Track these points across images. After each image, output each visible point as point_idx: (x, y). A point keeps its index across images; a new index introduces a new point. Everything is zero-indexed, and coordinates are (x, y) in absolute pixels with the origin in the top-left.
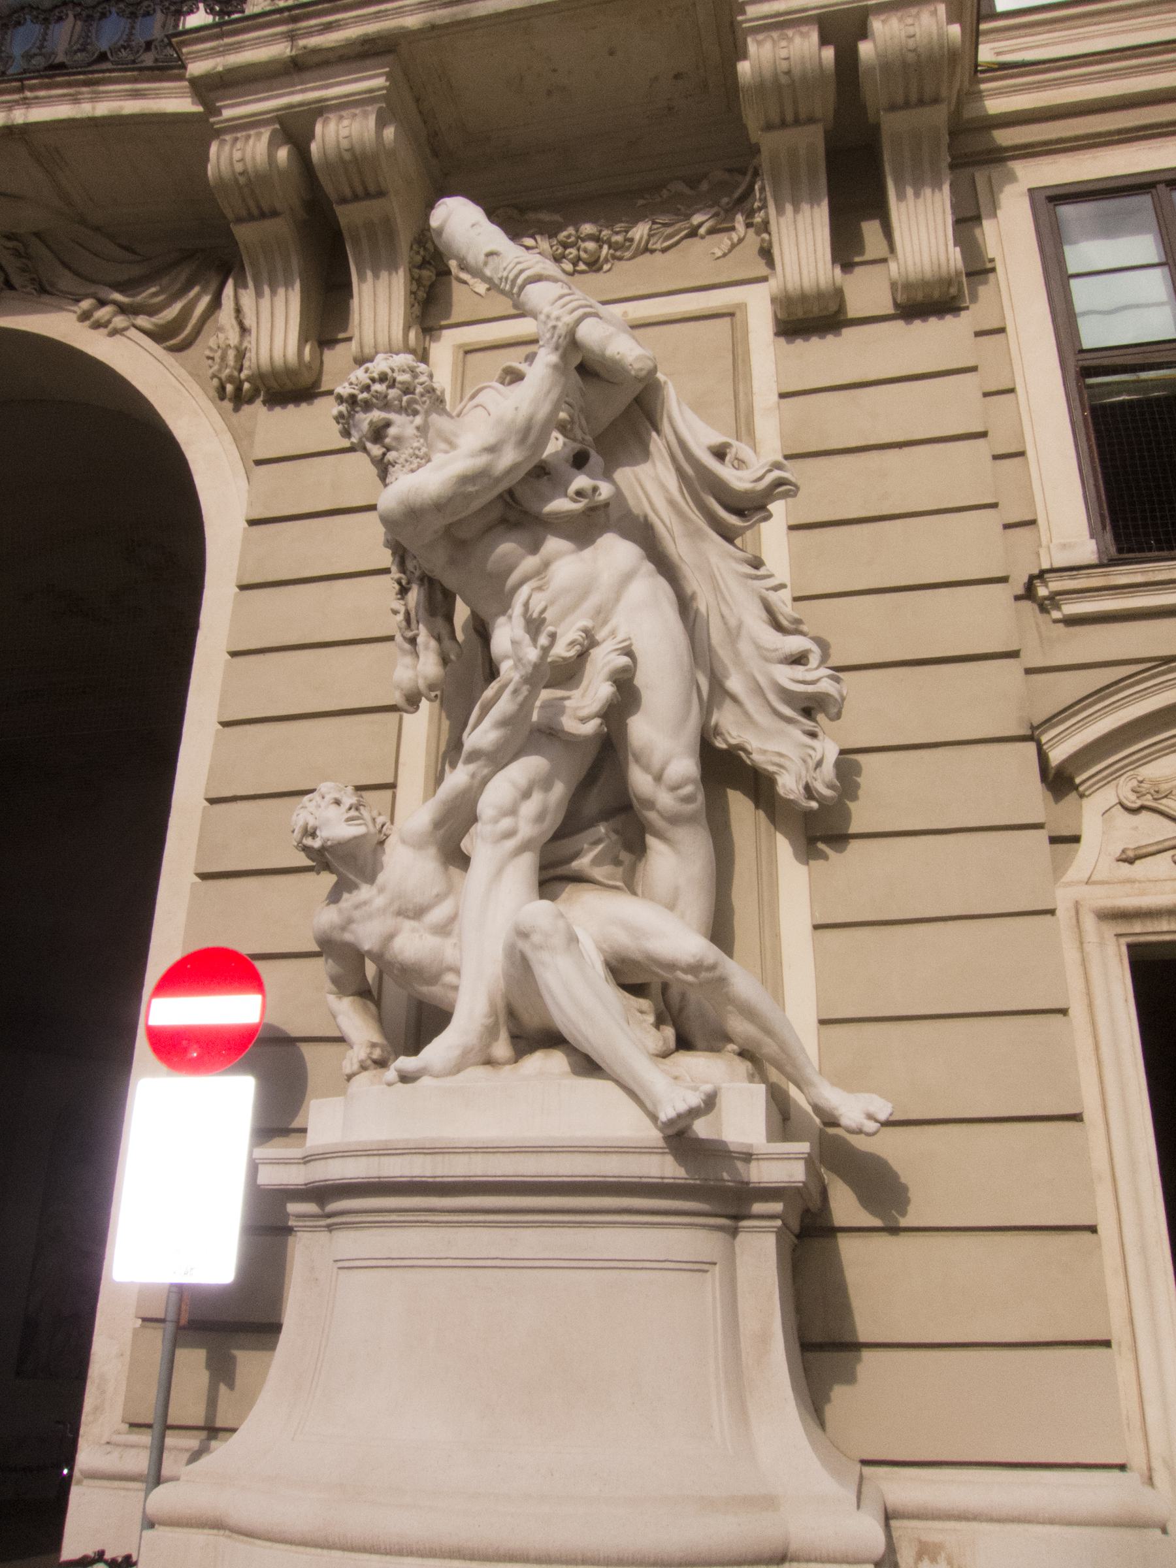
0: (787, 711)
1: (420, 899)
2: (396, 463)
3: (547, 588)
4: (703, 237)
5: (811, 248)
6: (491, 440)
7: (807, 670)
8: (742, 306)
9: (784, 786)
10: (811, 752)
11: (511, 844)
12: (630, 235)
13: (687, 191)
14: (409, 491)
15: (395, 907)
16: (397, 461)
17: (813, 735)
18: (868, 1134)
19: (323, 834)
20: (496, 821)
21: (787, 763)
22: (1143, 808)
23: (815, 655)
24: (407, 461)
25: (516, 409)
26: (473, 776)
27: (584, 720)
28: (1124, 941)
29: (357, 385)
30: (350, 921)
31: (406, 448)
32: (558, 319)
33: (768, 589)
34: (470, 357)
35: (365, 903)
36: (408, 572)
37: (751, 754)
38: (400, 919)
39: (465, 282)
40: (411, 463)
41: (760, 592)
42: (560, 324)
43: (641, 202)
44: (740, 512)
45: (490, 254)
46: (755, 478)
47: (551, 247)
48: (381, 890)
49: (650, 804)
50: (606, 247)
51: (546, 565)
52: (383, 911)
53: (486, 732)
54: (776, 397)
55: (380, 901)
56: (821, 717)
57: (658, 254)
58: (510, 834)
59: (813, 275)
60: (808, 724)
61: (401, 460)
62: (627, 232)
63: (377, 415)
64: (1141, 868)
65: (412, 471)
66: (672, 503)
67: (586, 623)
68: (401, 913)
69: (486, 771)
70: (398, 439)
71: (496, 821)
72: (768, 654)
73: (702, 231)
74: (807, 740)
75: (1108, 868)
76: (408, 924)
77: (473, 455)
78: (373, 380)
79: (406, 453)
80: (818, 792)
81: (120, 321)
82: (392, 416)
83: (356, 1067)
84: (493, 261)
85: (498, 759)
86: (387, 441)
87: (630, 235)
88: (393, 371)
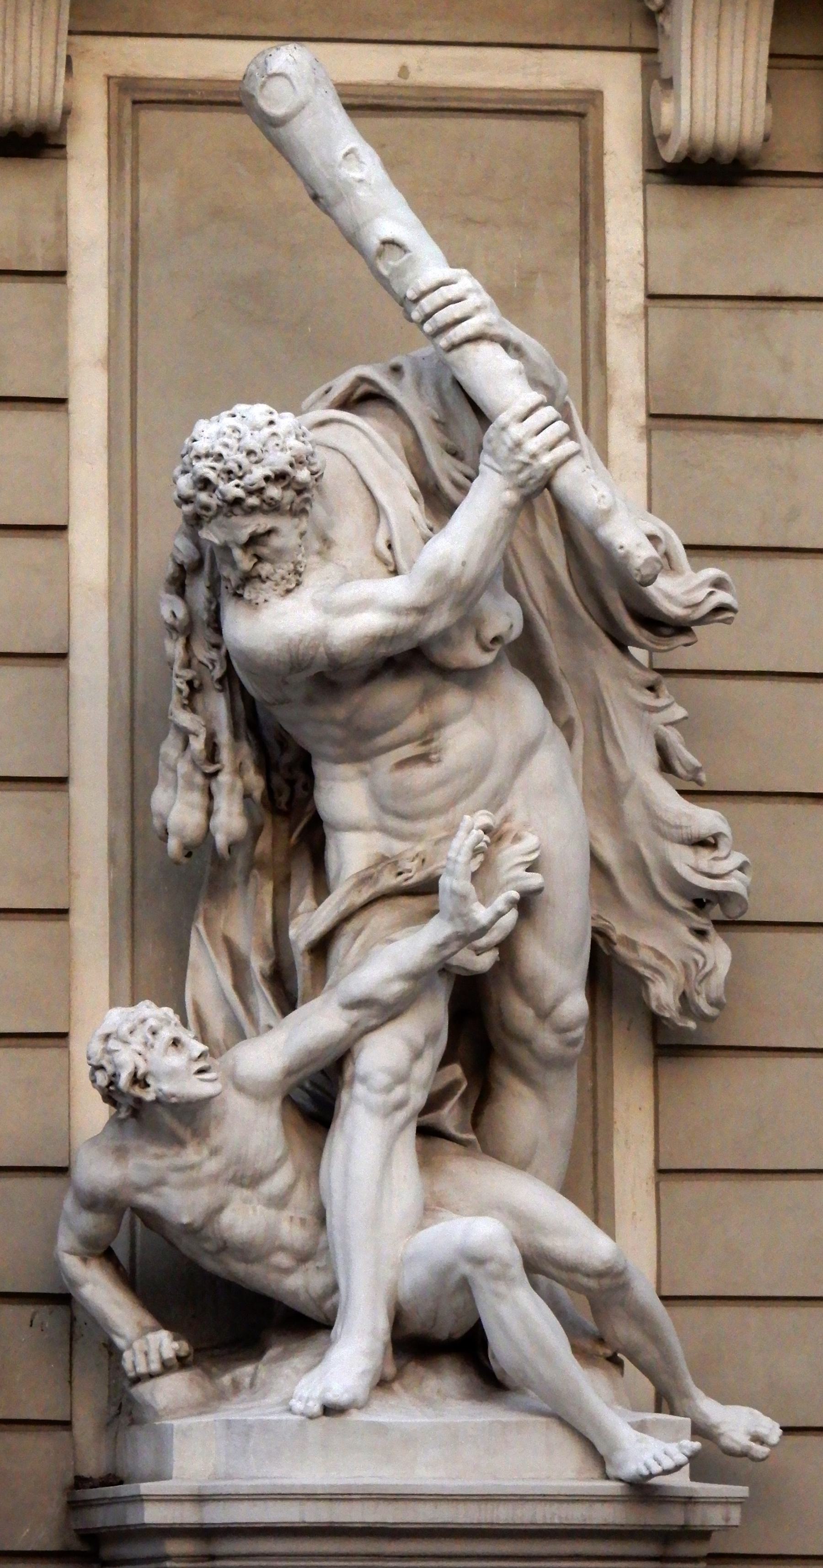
1: (262, 1164)
2: (267, 578)
3: (439, 761)
5: (737, 78)
6: (426, 599)
7: (715, 859)
8: (594, 97)
9: (658, 999)
10: (698, 957)
11: (401, 1116)
14: (301, 641)
15: (231, 1173)
16: (272, 578)
17: (701, 934)
18: (754, 1459)
20: (388, 1089)
21: (666, 968)
23: (726, 839)
24: (283, 578)
25: (464, 564)
26: (355, 1025)
27: (479, 951)
29: (241, 478)
30: (160, 1182)
31: (287, 562)
32: (534, 456)
33: (665, 725)
35: (192, 1167)
36: (195, 662)
37: (615, 944)
38: (231, 1187)
40: (288, 581)
41: (658, 729)
42: (536, 464)
45: (390, 243)
46: (687, 603)
49: (525, 1041)
51: (437, 726)
52: (215, 1178)
53: (389, 981)
54: (639, 298)
55: (212, 1166)
58: (400, 1105)
59: (735, 124)
61: (277, 577)
63: (260, 523)
65: (288, 591)
66: (552, 583)
67: (484, 818)
69: (373, 1022)
70: (280, 552)
71: (388, 1089)
72: (665, 828)
74: (693, 940)
76: (246, 1193)
78: (267, 479)
79: (284, 568)
80: (698, 1008)
82: (284, 524)
83: (155, 1367)
86: (264, 551)
88: (291, 465)
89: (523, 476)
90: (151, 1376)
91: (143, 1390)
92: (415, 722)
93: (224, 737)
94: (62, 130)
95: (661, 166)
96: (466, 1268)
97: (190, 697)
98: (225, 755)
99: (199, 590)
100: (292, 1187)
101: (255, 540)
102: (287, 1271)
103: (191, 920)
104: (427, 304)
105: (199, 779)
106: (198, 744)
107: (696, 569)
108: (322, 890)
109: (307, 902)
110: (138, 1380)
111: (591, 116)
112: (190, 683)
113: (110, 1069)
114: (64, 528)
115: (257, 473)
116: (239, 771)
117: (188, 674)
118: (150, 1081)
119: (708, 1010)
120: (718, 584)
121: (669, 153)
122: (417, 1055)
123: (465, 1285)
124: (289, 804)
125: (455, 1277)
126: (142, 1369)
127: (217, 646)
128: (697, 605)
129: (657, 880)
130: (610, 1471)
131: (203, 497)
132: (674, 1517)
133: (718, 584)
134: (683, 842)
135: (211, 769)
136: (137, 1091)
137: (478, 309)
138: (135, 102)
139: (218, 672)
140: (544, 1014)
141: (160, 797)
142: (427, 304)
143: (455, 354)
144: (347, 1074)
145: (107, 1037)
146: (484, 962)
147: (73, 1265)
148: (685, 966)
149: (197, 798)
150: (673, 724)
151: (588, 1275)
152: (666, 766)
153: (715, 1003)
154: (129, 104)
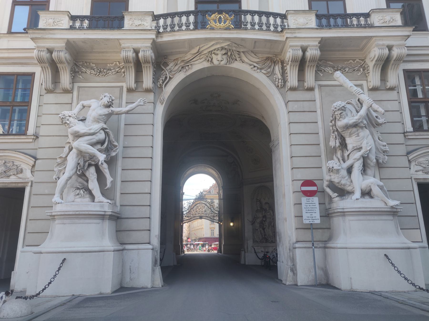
0: (381, 152)
4: (356, 71)
6: (359, 118)
8: (362, 84)
12: (345, 69)
13: (353, 62)
17: (384, 155)
19: (335, 168)
21: (381, 159)
22: (419, 165)
27: (365, 154)
28: (416, 182)
30: (335, 178)
34: (322, 87)
39: (318, 73)
43: (346, 63)
44: (377, 125)
47: (333, 70)
48: (340, 175)
49: (369, 164)
50: (342, 71)
55: (340, 176)
56: (385, 153)
57: (349, 73)
58: (359, 169)
60: (384, 154)
62: (345, 69)
64: (418, 173)
65: (344, 119)
68: (342, 178)
73: (356, 70)
75: (414, 173)
76: (344, 179)
77: (356, 119)
80: (384, 162)
81: (258, 70)
82: (343, 112)
83: (335, 197)
84: (351, 88)
85: (358, 160)
87: (345, 69)
89: (369, 105)
90: (335, 198)
91: (334, 199)
92: (357, 133)
93: (337, 136)
94: (314, 88)
95: (369, 89)
96: (370, 184)
97: (333, 132)
98: (337, 138)
99: (333, 122)
100: (348, 179)
101: (340, 114)
102: (348, 187)
103: (333, 155)
104: (356, 91)
105: (335, 140)
106: (334, 137)
107: (382, 119)
108: (348, 151)
109: (346, 151)
110: (333, 198)
111: (362, 86)
112: (333, 131)
113: (329, 167)
114: (317, 122)
115: (341, 106)
116: (338, 139)
117: (333, 130)
118: (334, 167)
119: (385, 162)
120: (385, 120)
121: (370, 88)
122: (361, 164)
123: (370, 186)
124: (342, 144)
125: (369, 185)
126: (334, 197)
127: (335, 127)
128: (383, 122)
129: (380, 150)
130: (388, 205)
131: (335, 109)
132: (395, 210)
133: (385, 120)
134: (382, 146)
135: (336, 139)
136: (332, 169)
137: (361, 91)
138: (320, 86)
139: (336, 130)
140: (372, 161)
141: (330, 143)
142: (356, 91)
143: (359, 95)
144: (353, 167)
145: (329, 164)
146: (366, 155)
147: (325, 188)
148: (383, 158)
149: (334, 142)
150: (379, 135)
151: (380, 186)
152: (379, 139)
153: (386, 162)
154: (320, 87)
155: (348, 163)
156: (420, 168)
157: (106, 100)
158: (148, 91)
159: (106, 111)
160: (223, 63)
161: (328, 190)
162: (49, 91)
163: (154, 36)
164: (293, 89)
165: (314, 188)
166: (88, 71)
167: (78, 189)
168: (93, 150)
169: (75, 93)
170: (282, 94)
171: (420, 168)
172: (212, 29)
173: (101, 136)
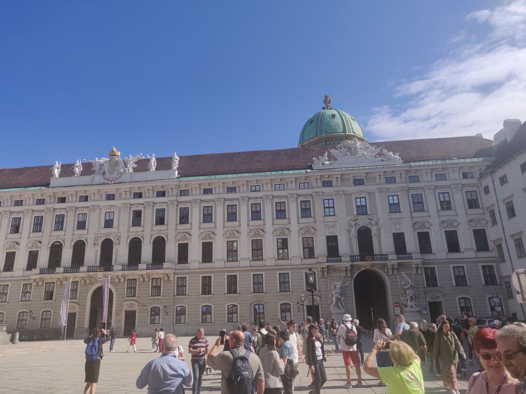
155: (407, 298)
156: (429, 298)
157: (341, 283)
158: (349, 277)
159: (341, 286)
160: (370, 268)
161: (402, 305)
162: (321, 278)
163: (351, 264)
164: (391, 275)
165: (398, 305)
166: (331, 271)
167: (336, 306)
168: (339, 296)
169: (328, 277)
170: (387, 276)
171: (429, 298)
172: (367, 261)
173: (341, 292)
